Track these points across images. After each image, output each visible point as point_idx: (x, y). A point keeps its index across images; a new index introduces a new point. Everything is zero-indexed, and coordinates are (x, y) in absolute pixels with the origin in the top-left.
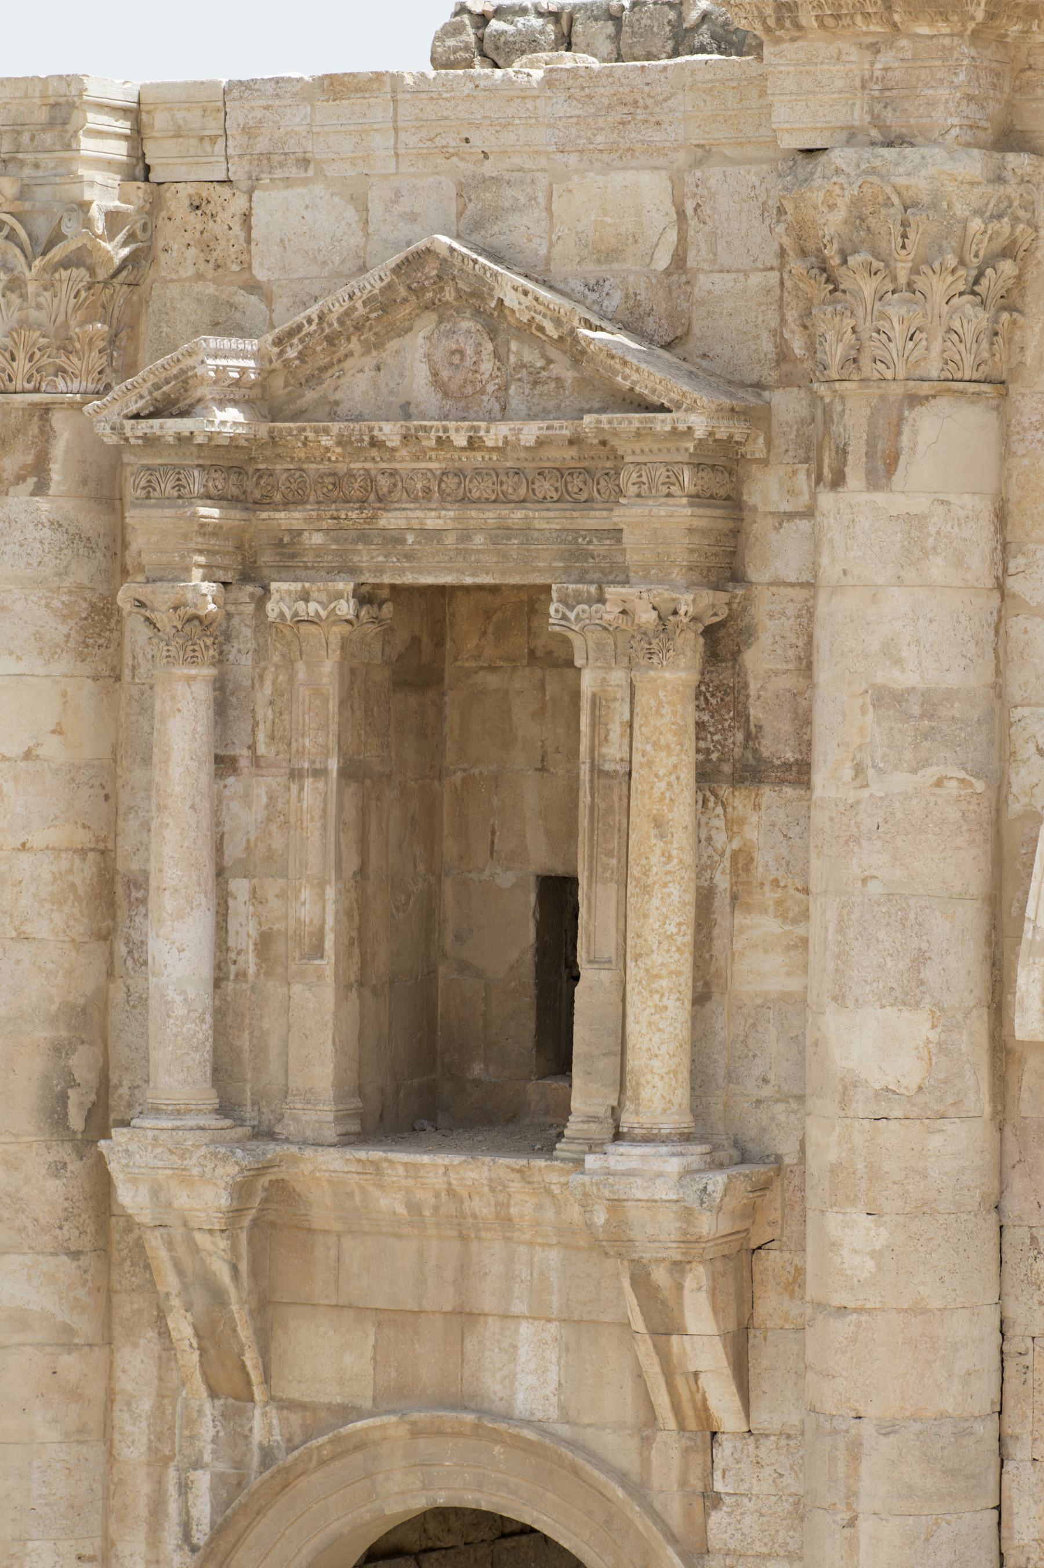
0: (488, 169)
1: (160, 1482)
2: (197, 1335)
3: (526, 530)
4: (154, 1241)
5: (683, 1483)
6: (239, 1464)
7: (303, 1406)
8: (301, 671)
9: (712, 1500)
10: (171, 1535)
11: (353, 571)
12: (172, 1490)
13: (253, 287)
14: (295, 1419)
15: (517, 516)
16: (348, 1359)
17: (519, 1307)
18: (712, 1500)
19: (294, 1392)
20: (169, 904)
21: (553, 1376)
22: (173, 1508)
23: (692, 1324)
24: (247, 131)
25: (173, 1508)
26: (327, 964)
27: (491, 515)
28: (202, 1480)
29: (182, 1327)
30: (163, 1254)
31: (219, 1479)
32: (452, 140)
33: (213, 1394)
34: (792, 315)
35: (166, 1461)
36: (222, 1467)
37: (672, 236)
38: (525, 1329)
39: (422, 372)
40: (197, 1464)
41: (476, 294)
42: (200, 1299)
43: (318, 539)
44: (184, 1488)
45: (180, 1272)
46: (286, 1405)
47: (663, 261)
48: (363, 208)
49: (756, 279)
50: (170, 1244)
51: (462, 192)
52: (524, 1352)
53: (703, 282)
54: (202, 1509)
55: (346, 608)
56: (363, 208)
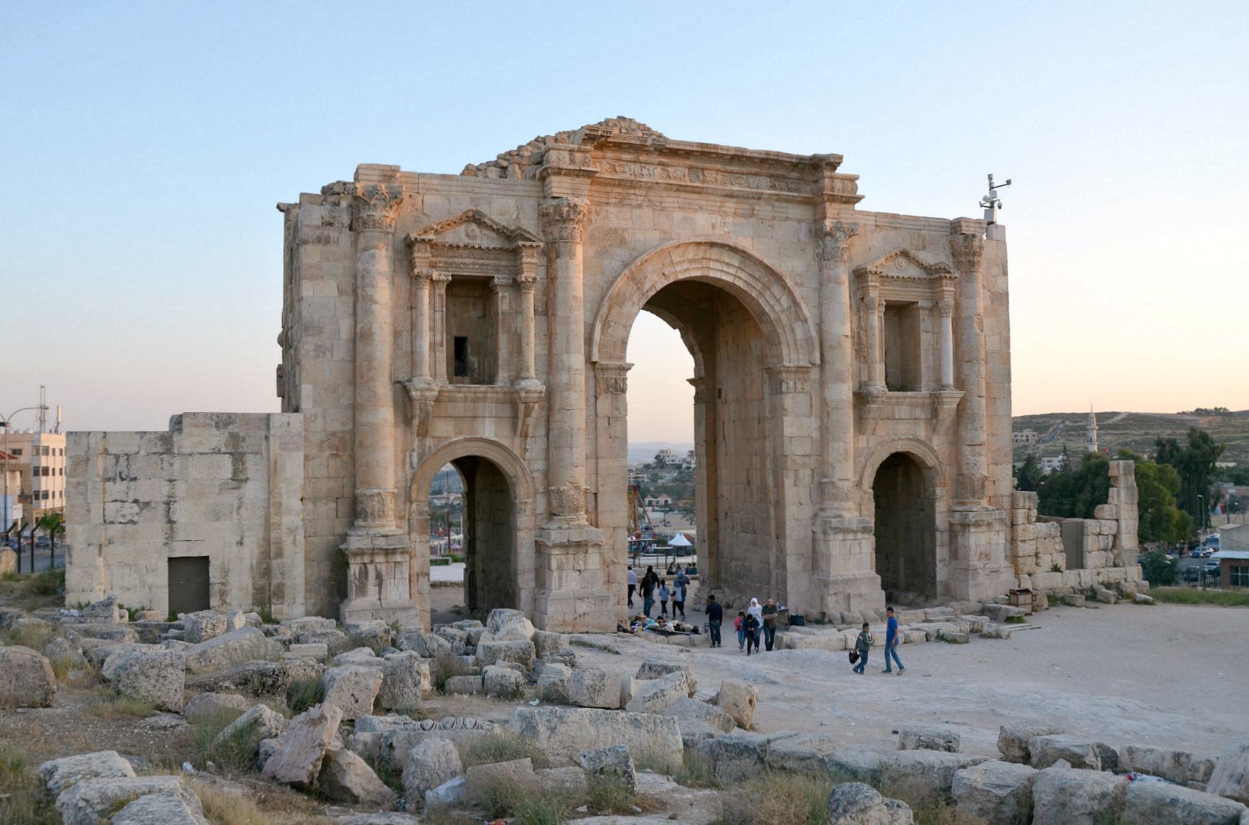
0: (477, 196)
1: (405, 456)
2: (419, 423)
3: (488, 265)
4: (417, 405)
5: (520, 448)
6: (424, 450)
7: (438, 438)
8: (437, 291)
9: (526, 450)
10: (408, 466)
11: (449, 271)
12: (408, 456)
13: (424, 214)
14: (436, 440)
15: (486, 262)
16: (448, 427)
17: (487, 415)
18: (526, 450)
19: (436, 435)
20: (424, 334)
21: (493, 428)
22: (408, 460)
23: (533, 415)
24: (424, 183)
25: (408, 460)
26: (444, 349)
27: (480, 262)
28: (415, 454)
29: (416, 422)
30: (418, 406)
31: (419, 453)
32: (469, 189)
33: (418, 436)
34: (540, 229)
35: (406, 451)
36: (420, 451)
37: (516, 212)
38: (487, 419)
39: (464, 233)
40: (414, 450)
41: (479, 220)
42: (423, 415)
43: (441, 265)
44: (411, 456)
45: (420, 409)
46: (434, 437)
47: (514, 217)
48: (449, 201)
49: (533, 222)
50: (420, 404)
51: (472, 199)
52: (487, 424)
53: (522, 221)
54: (415, 460)
55: (450, 278)
56: (449, 201)
